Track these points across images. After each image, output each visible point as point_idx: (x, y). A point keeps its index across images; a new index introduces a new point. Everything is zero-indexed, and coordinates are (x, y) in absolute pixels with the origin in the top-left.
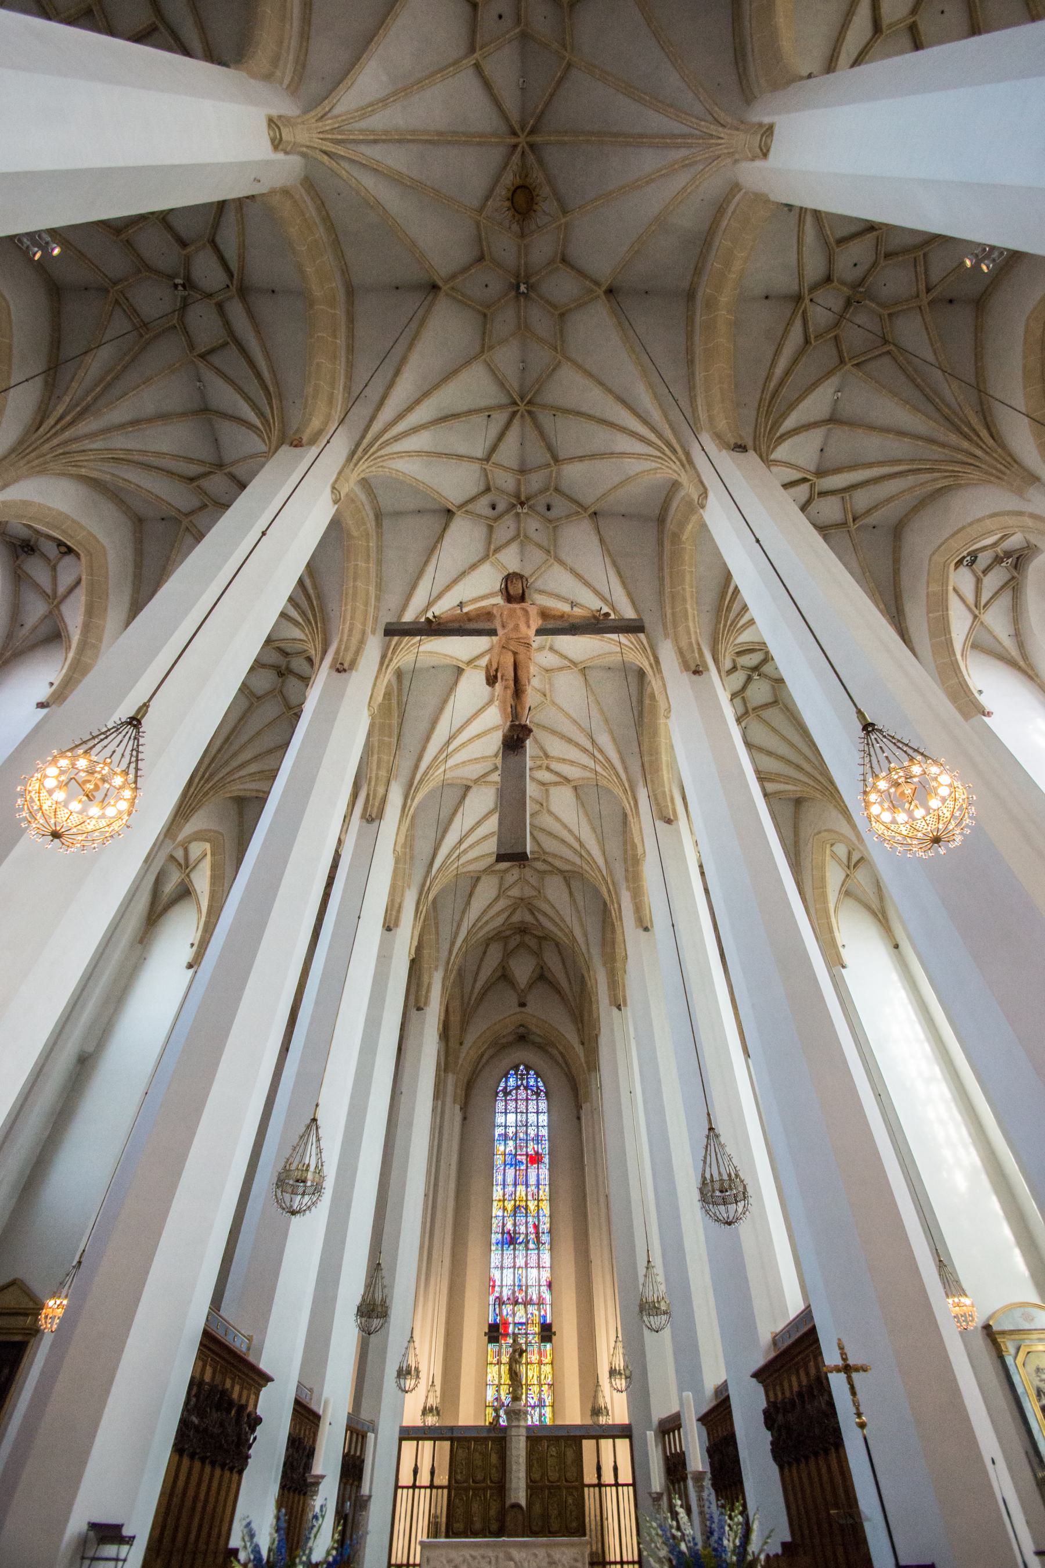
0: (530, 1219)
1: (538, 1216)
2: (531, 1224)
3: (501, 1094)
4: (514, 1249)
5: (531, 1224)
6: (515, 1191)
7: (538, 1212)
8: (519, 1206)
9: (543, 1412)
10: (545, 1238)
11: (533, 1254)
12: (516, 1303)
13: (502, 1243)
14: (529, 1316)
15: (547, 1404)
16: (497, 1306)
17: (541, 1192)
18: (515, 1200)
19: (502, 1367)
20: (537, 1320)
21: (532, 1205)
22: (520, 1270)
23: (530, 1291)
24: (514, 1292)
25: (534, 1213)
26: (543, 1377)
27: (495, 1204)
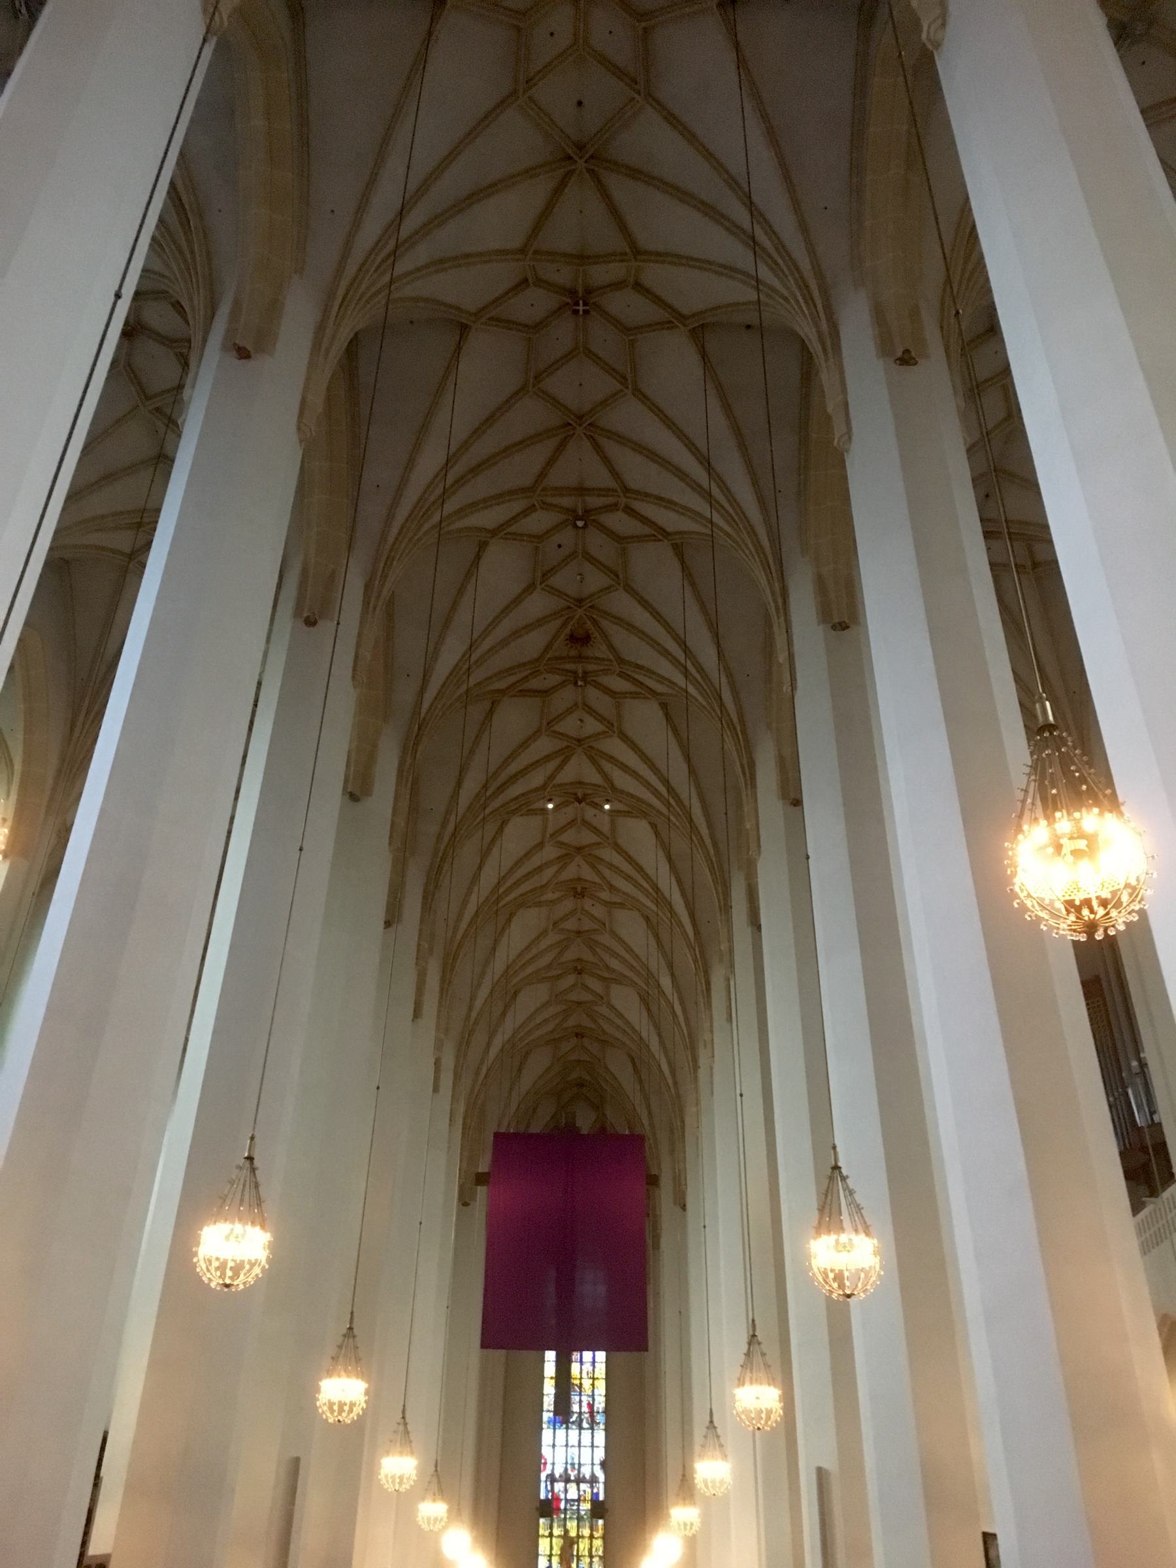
0: (584, 1399)
1: (593, 1395)
2: (584, 1404)
4: (567, 1428)
5: (584, 1404)
7: (593, 1391)
10: (600, 1418)
11: (586, 1434)
12: (567, 1480)
13: (554, 1423)
14: (582, 1493)
16: (548, 1483)
19: (554, 1540)
20: (589, 1497)
21: (587, 1383)
24: (566, 1469)
26: (594, 1550)
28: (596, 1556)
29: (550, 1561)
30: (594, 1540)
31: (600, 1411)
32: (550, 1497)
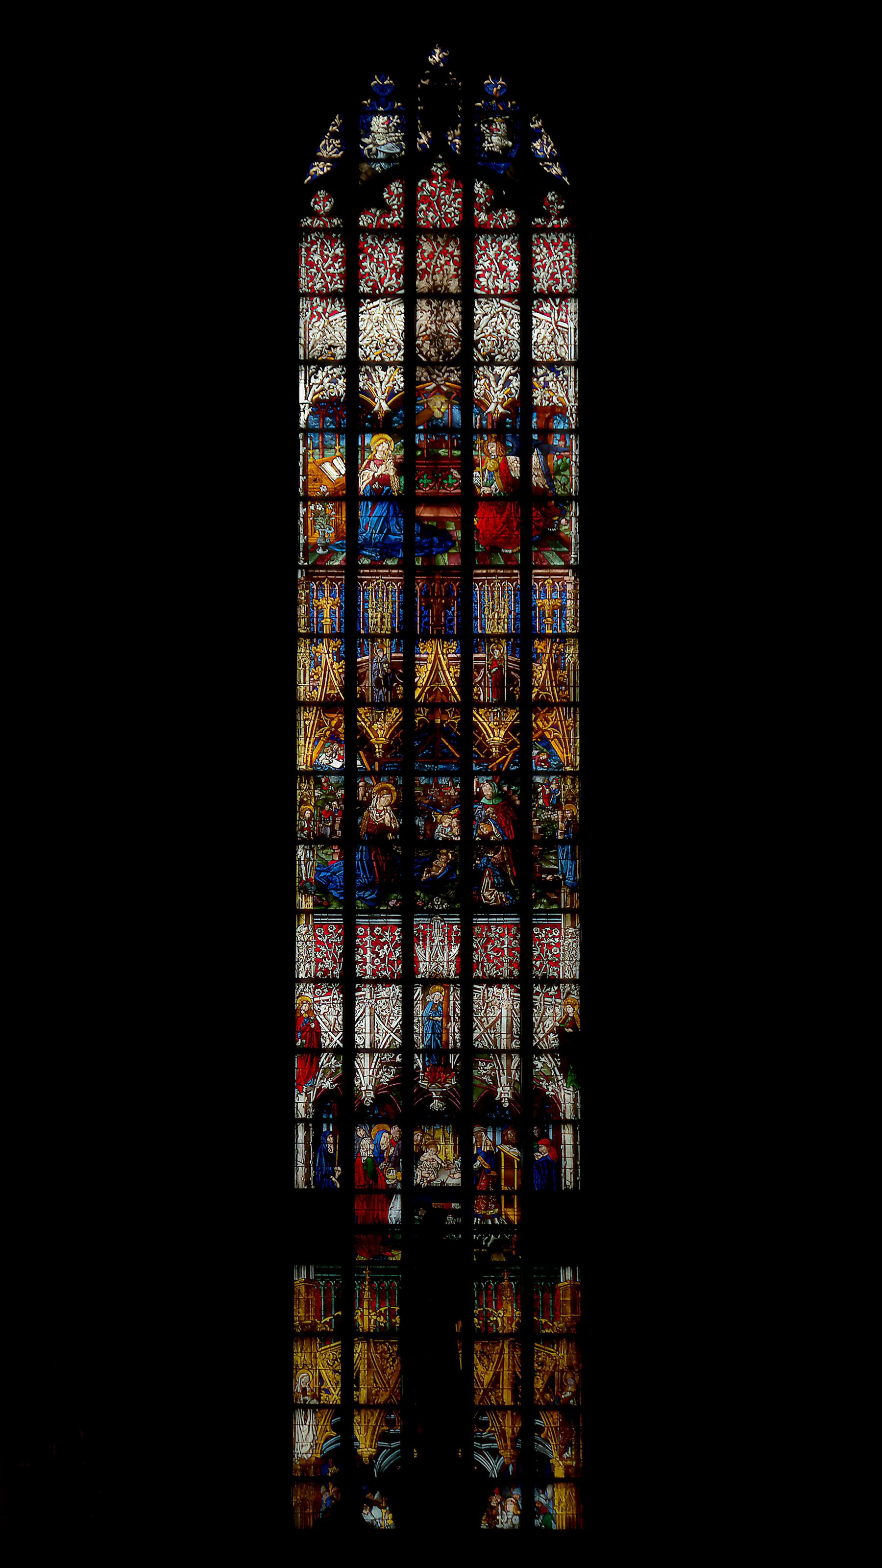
3: (323, 203)
6: (409, 666)
7: (524, 756)
9: (540, 1499)
15: (559, 1473)
17: (540, 671)
18: (408, 704)
22: (436, 995)
23: (483, 1070)
25: (507, 761)
26: (539, 1384)
27: (307, 719)
29: (344, 1429)
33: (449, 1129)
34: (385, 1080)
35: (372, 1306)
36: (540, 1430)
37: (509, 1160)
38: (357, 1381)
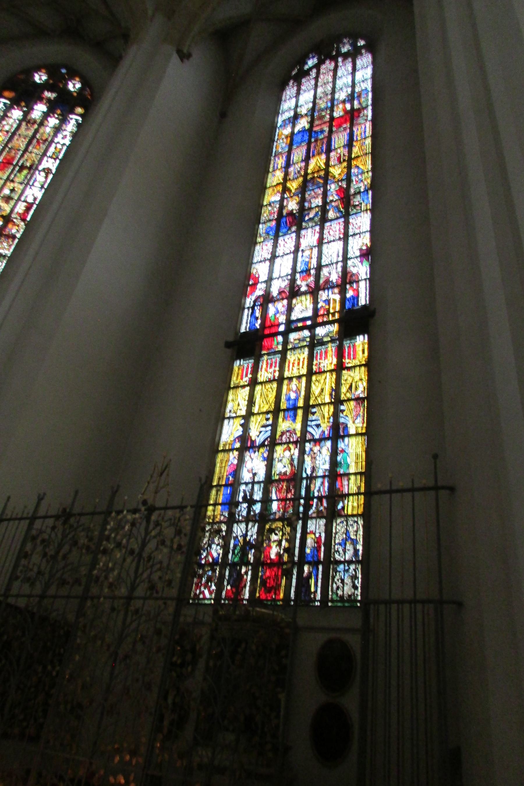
8: (313, 178)
15: (352, 431)
28: (349, 400)
30: (344, 372)
31: (362, 190)
32: (258, 326)
33: (308, 297)
34: (283, 286)
35: (266, 371)
36: (343, 411)
37: (335, 301)
38: (254, 403)
